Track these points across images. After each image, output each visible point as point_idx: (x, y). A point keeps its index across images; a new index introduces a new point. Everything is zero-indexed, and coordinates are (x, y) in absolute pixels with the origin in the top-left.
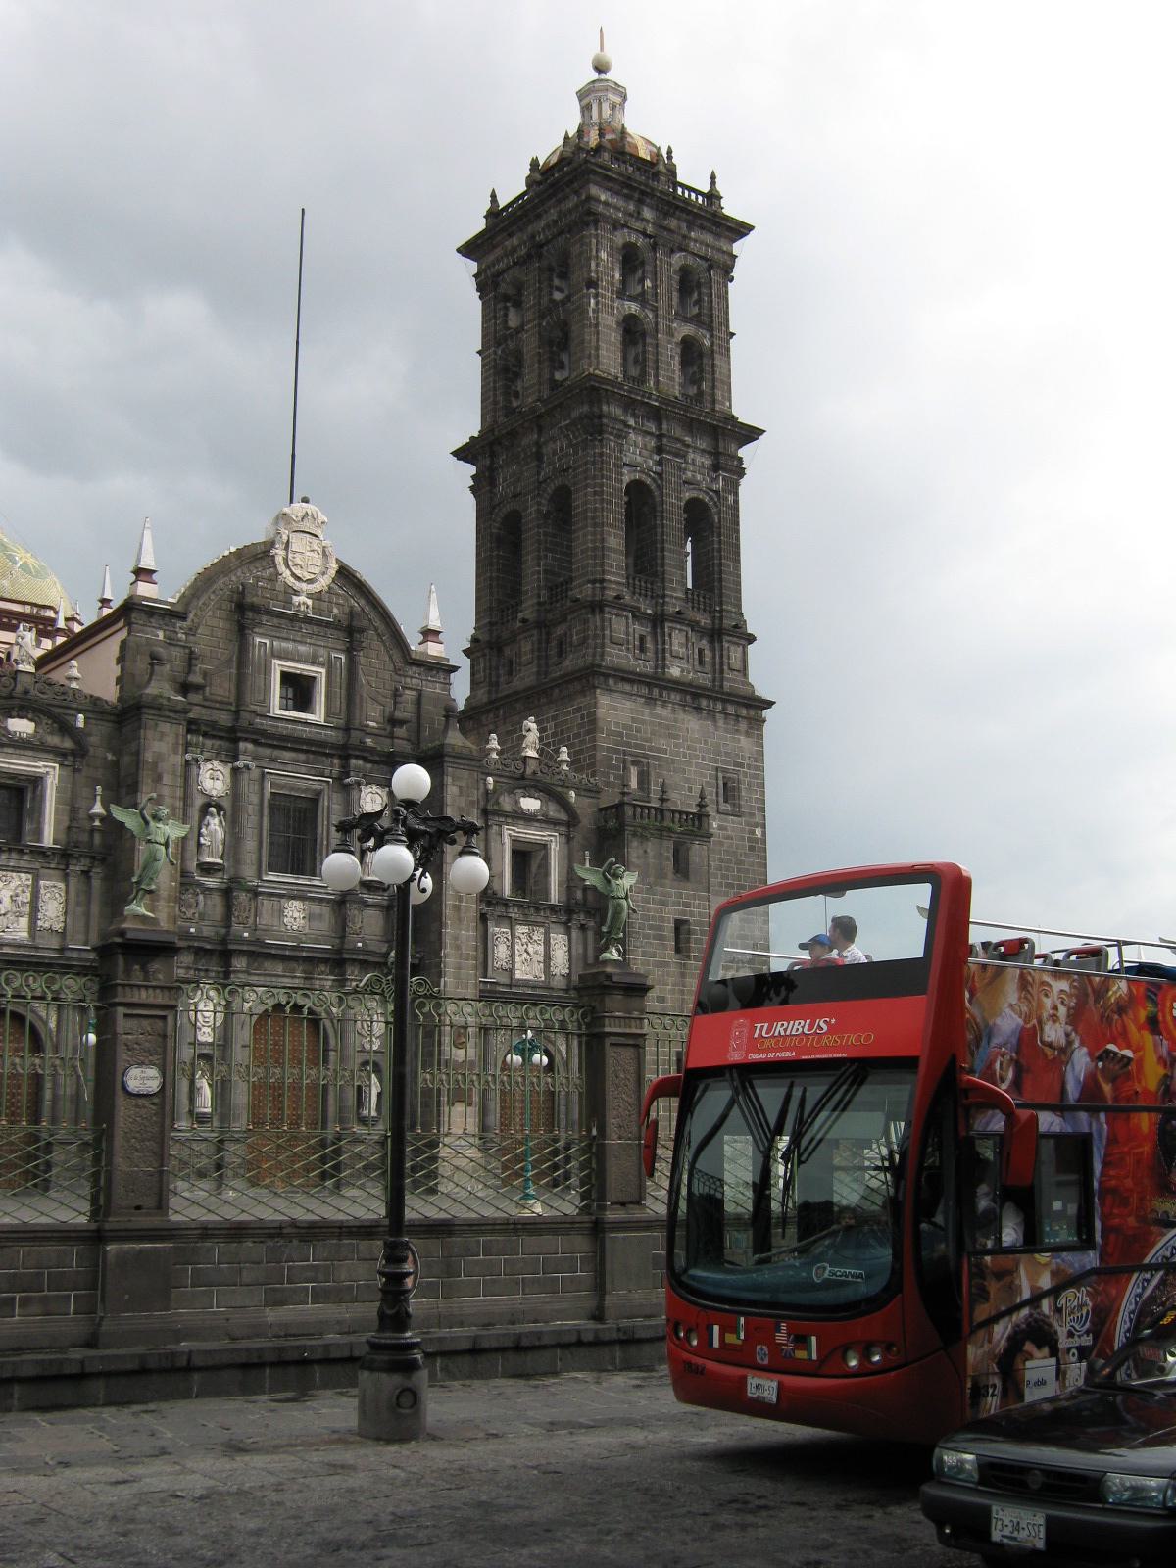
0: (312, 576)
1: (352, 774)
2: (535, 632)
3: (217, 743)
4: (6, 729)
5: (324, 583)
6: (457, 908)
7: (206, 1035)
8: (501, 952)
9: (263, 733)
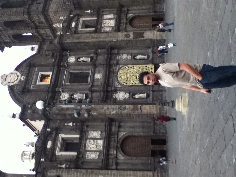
0: (17, 76)
1: (64, 65)
2: (38, 30)
3: (56, 96)
4: (50, 148)
5: (19, 74)
6: (97, 38)
7: (127, 96)
8: (108, 29)
9: (53, 85)
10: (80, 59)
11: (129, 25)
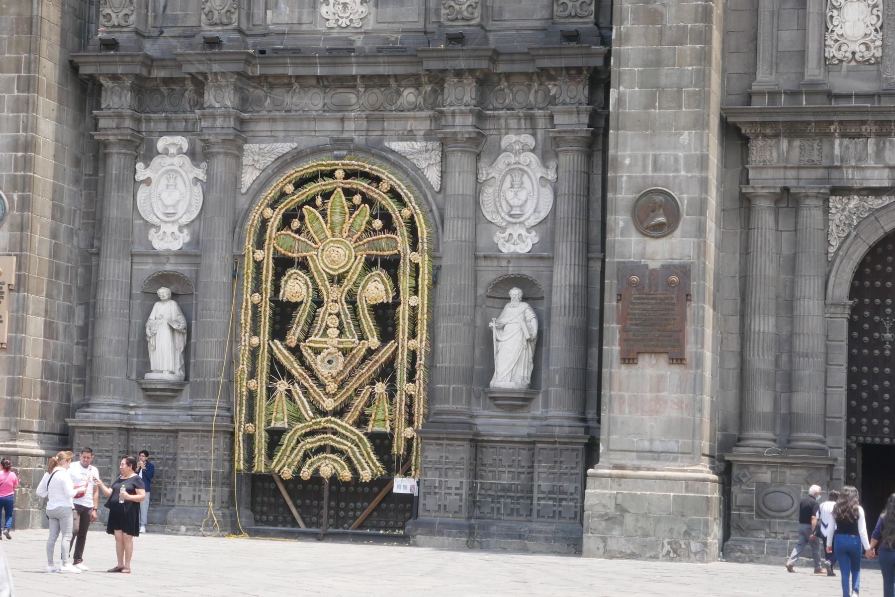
7: (169, 239)
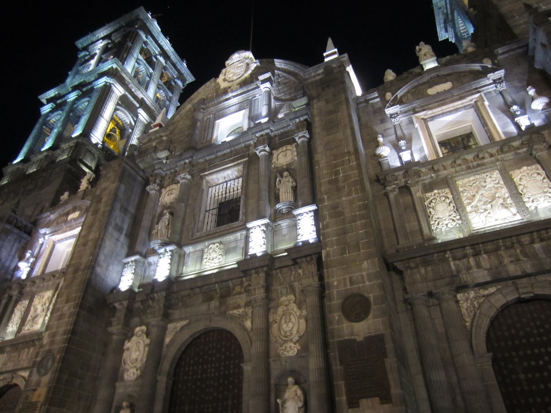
7: (131, 374)
10: (286, 177)
11: (499, 301)
